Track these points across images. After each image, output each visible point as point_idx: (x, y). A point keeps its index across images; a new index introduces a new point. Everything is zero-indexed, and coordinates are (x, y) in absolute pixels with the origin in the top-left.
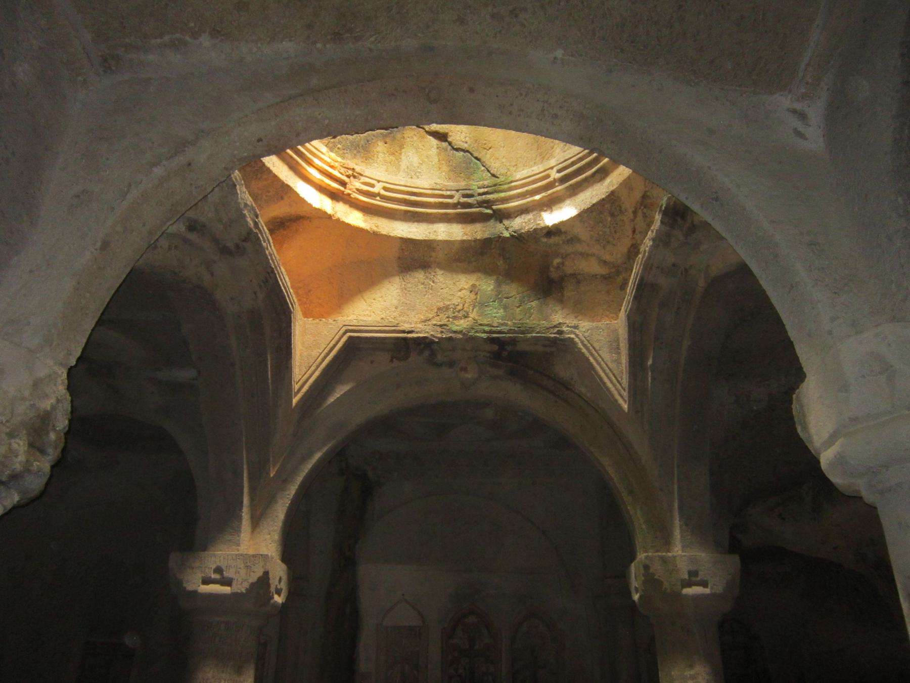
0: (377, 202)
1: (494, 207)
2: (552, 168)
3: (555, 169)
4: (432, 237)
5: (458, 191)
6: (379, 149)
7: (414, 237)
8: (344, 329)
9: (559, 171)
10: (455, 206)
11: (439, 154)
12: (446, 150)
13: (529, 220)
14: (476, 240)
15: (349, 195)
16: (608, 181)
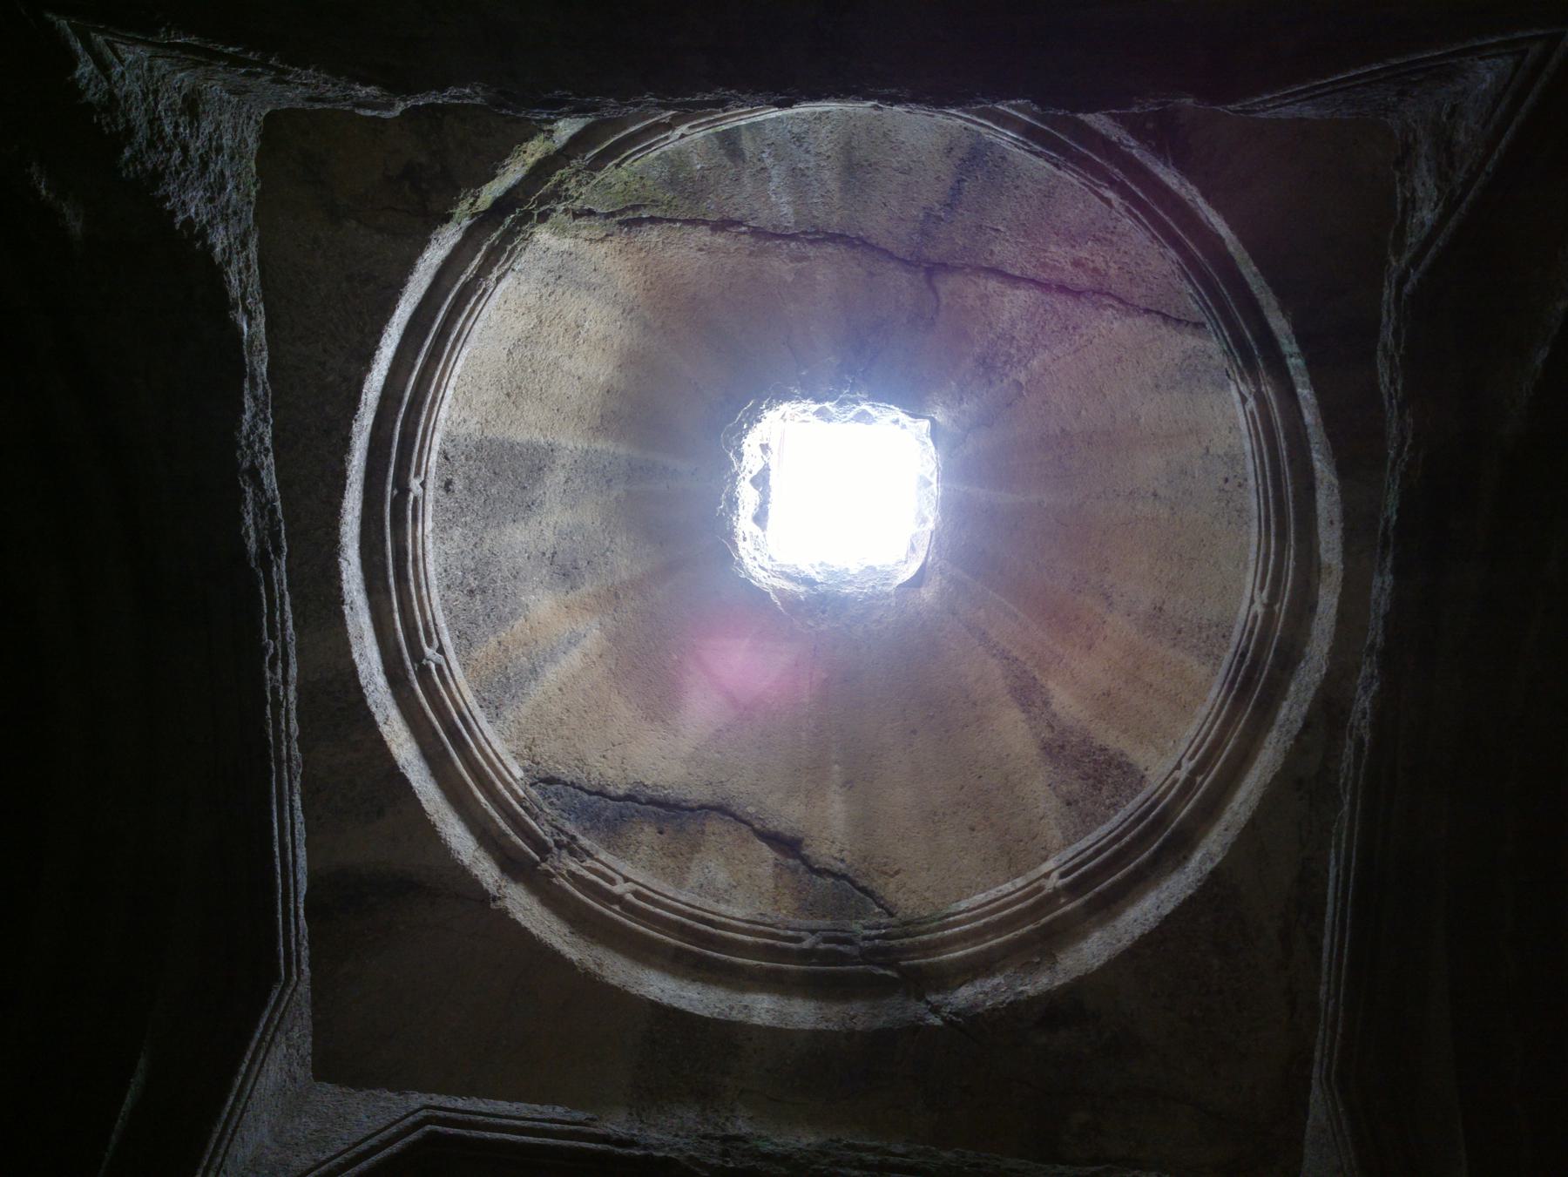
0: (613, 913)
1: (903, 963)
2: (1047, 875)
3: (1055, 874)
4: (736, 1016)
5: (813, 932)
6: (642, 837)
7: (690, 1009)
8: (423, 1113)
9: (1062, 876)
10: (806, 956)
11: (777, 876)
12: (795, 871)
13: (996, 988)
14: (851, 1034)
15: (548, 874)
16: (1198, 856)
